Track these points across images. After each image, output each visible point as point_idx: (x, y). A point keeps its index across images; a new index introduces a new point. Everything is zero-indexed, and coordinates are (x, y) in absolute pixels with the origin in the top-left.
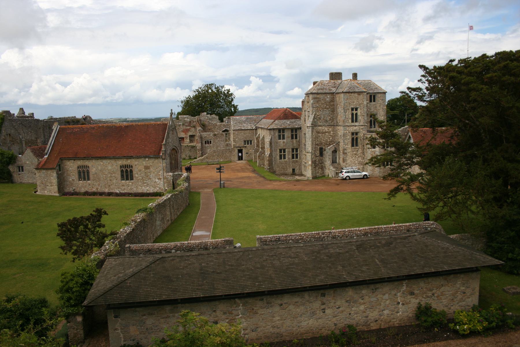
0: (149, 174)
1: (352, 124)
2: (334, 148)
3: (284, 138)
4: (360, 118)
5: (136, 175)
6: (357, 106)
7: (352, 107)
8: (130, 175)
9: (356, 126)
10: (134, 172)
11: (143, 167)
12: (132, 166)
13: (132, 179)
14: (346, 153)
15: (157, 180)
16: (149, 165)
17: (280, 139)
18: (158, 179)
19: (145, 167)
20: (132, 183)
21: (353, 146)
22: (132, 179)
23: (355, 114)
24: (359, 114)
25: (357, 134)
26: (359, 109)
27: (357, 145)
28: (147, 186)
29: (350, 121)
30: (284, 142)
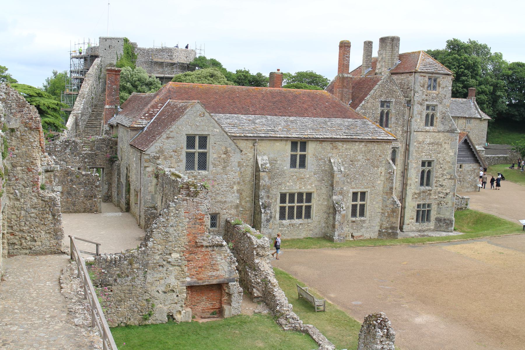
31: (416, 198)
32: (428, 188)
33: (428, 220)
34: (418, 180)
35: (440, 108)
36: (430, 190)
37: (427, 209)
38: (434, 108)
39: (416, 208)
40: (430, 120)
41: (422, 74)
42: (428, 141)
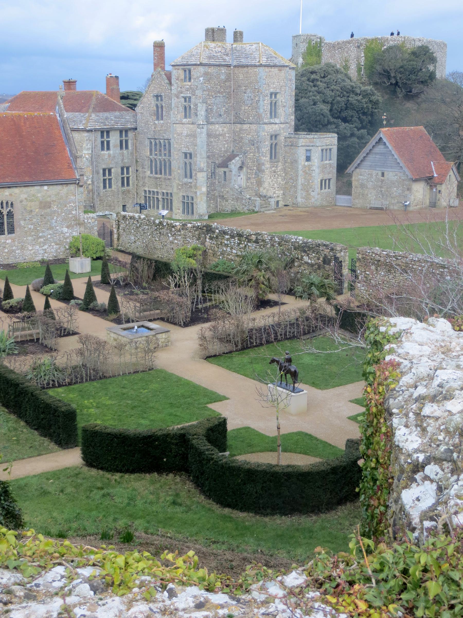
0: (49, 218)
2: (240, 162)
3: (108, 149)
4: (280, 111)
5: (22, 223)
6: (278, 91)
7: (272, 90)
8: (8, 223)
9: (276, 124)
10: (17, 216)
11: (37, 203)
12: (12, 204)
13: (11, 231)
15: (65, 230)
16: (48, 199)
17: (103, 149)
18: (68, 227)
19: (41, 203)
20: (13, 240)
21: (271, 158)
22: (11, 231)
28: (45, 244)
29: (269, 114)
30: (109, 155)
31: (179, 189)
32: (190, 180)
33: (193, 213)
34: (182, 172)
35: (193, 100)
36: (191, 183)
37: (190, 201)
38: (190, 98)
39: (181, 199)
40: (187, 111)
41: (177, 67)
42: (185, 133)
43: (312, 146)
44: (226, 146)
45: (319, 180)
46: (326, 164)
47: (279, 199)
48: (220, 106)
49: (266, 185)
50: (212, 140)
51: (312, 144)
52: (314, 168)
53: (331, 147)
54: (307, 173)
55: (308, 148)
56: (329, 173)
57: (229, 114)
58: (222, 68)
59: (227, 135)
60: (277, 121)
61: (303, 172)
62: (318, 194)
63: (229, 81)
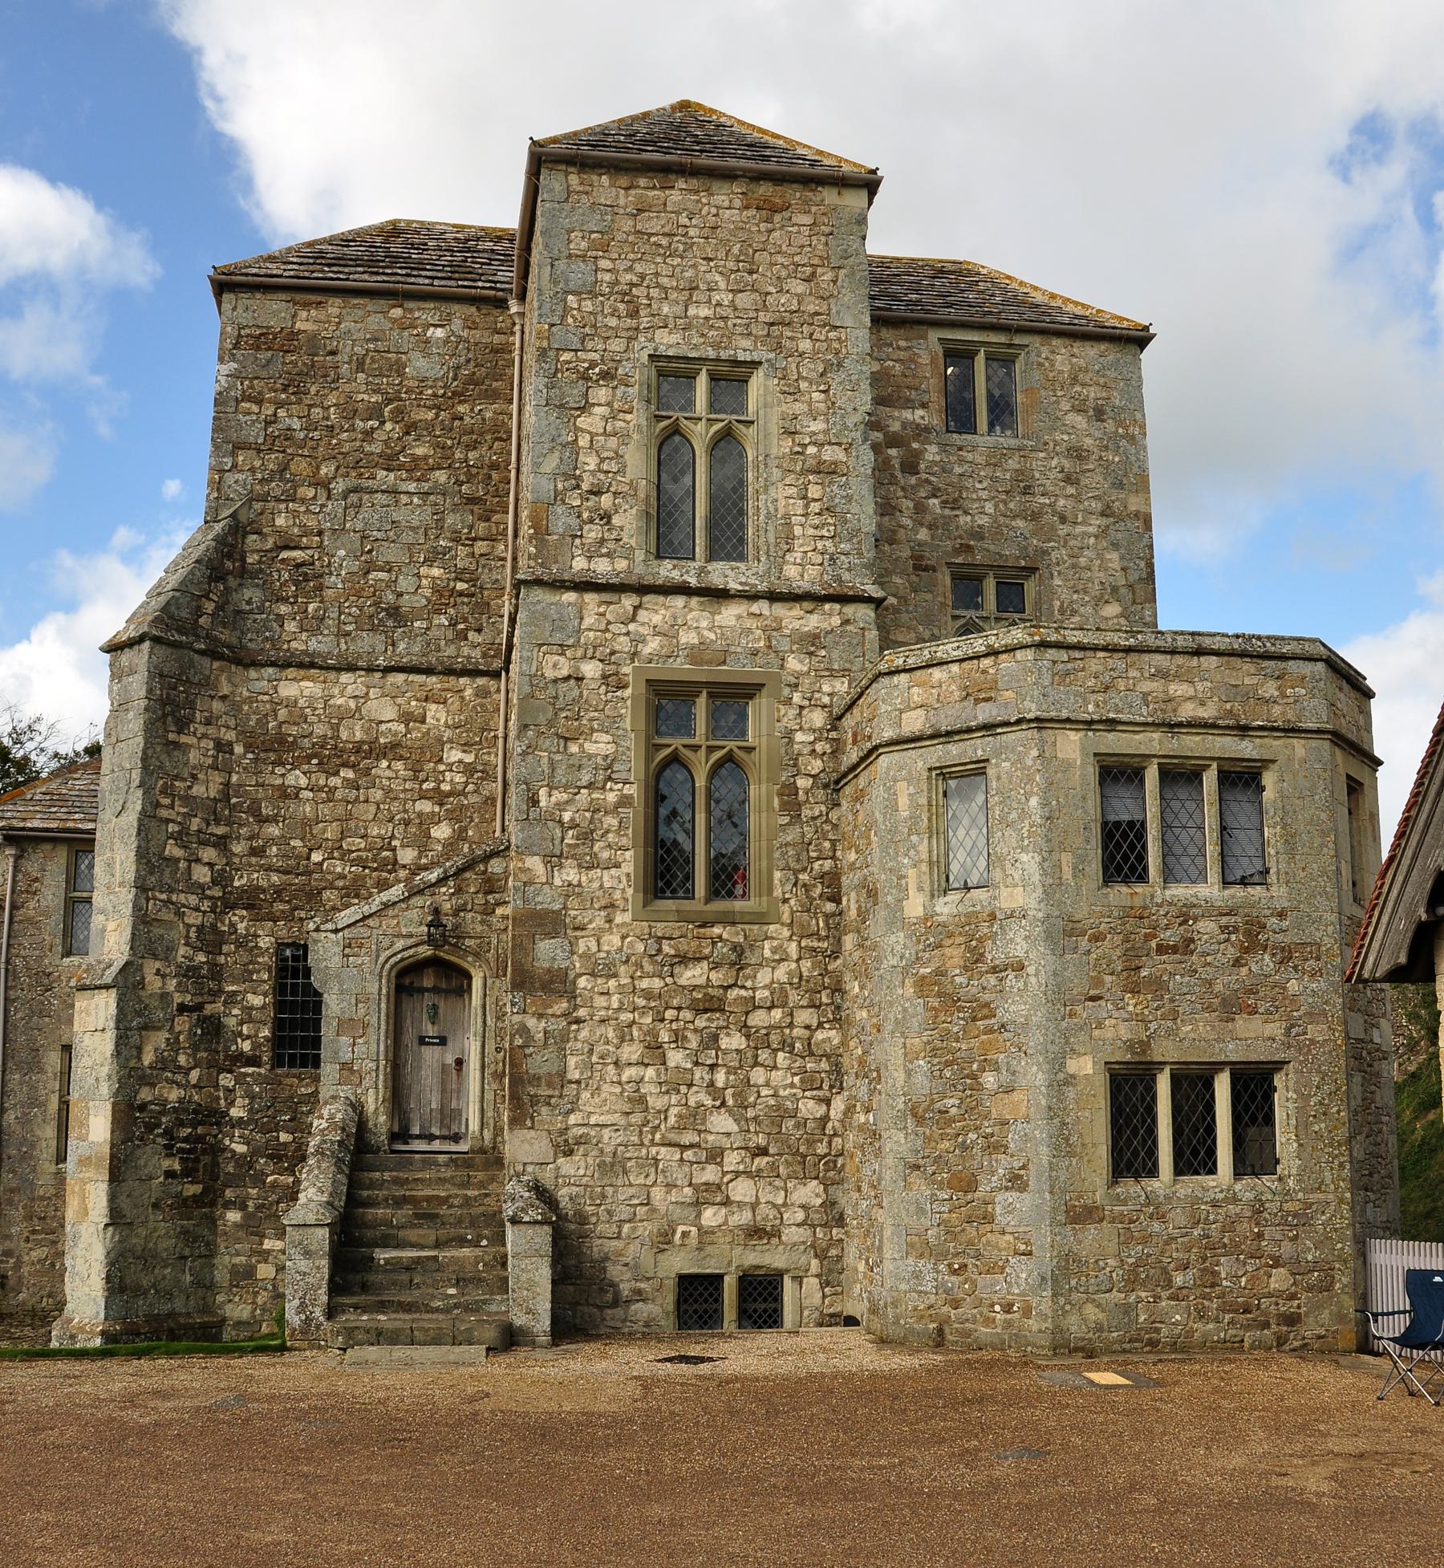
1: (668, 571)
2: (413, 922)
4: (774, 498)
7: (668, 341)
9: (721, 595)
14: (558, 984)
23: (700, 434)
24: (763, 443)
25: (734, 697)
26: (757, 384)
27: (727, 877)
29: (628, 521)
43: (988, 728)
44: (442, 832)
45: (1085, 1066)
46: (1186, 914)
47: (772, 1258)
48: (390, 553)
49: (598, 1110)
50: (297, 778)
51: (985, 713)
52: (1018, 943)
53: (1246, 748)
54: (951, 1001)
55: (954, 752)
56: (1231, 1007)
57: (484, 607)
58: (426, 313)
59: (454, 755)
60: (722, 574)
61: (922, 983)
62: (1081, 1215)
63: (492, 396)
